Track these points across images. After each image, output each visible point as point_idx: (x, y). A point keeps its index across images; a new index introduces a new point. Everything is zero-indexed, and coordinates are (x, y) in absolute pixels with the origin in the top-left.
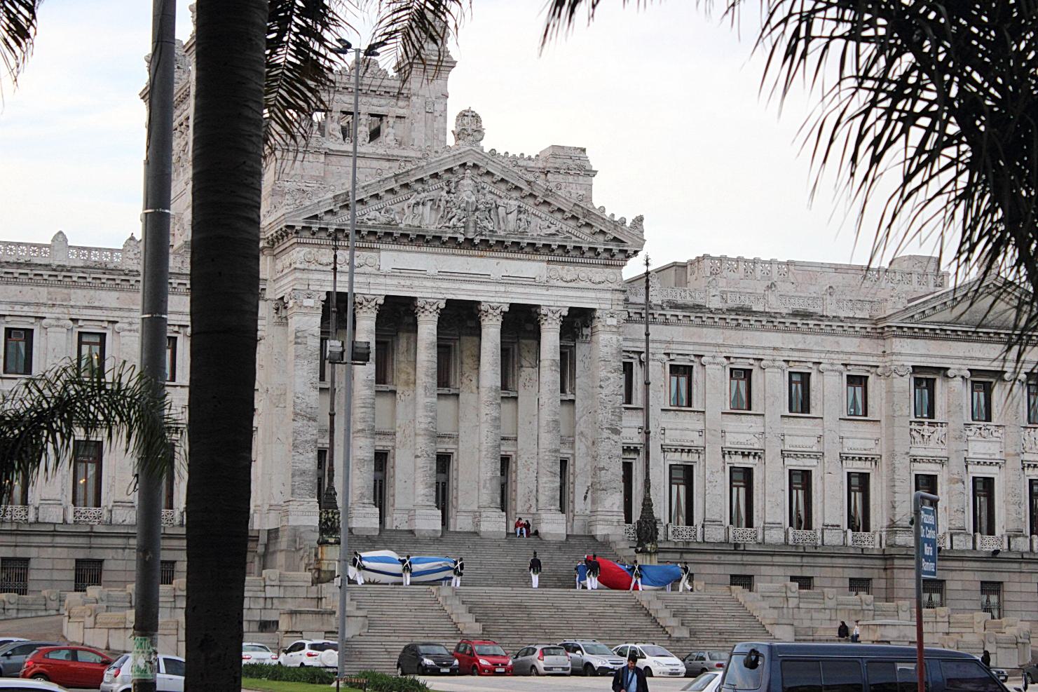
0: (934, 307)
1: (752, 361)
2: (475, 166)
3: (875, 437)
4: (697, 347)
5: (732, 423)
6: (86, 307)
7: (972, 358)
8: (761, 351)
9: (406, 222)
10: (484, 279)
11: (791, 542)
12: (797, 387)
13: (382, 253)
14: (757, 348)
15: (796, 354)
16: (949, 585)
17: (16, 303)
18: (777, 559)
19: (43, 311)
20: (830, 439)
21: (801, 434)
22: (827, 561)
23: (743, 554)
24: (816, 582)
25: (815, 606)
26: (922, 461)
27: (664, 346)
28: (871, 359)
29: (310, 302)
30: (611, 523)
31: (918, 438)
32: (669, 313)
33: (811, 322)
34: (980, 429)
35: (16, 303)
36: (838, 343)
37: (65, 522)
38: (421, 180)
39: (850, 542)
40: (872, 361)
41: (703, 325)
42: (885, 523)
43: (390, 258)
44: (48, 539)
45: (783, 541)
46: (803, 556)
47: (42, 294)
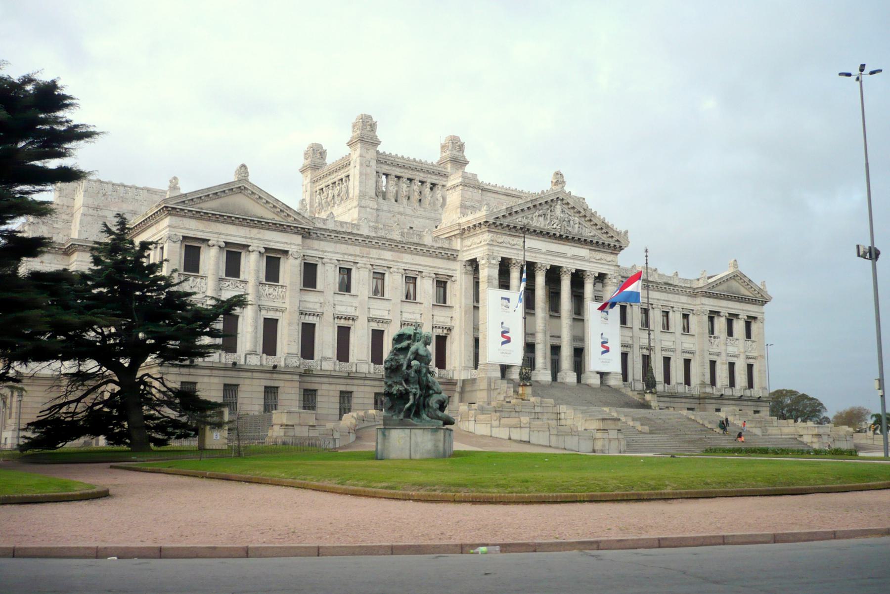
2: (563, 199)
10: (563, 255)
17: (345, 254)
19: (358, 260)
29: (494, 262)
35: (345, 254)
37: (369, 373)
38: (540, 204)
40: (691, 307)
42: (698, 382)
44: (361, 382)
47: (357, 250)
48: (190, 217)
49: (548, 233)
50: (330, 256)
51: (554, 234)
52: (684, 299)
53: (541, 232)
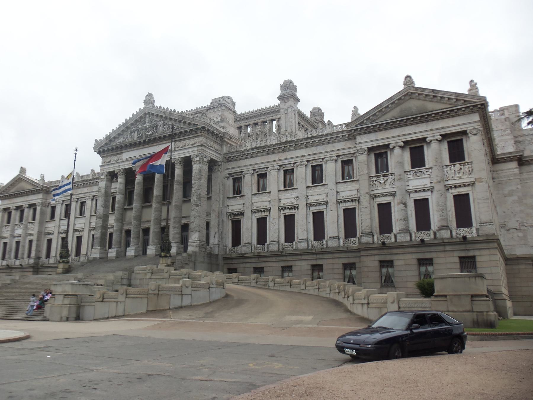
0: (375, 114)
1: (292, 165)
2: (149, 113)
3: (357, 188)
4: (266, 164)
5: (283, 195)
6: (80, 194)
7: (403, 135)
8: (295, 159)
9: (129, 140)
11: (310, 248)
12: (318, 173)
13: (124, 154)
14: (293, 158)
15: (312, 156)
16: (396, 263)
18: (304, 257)
20: (333, 193)
21: (317, 194)
22: (329, 256)
23: (286, 256)
24: (325, 267)
25: (159, 277)
26: (379, 196)
27: (252, 167)
28: (352, 150)
30: (193, 246)
31: (379, 185)
32: (251, 152)
33: (316, 140)
34: (416, 172)
36: (333, 146)
38: (132, 124)
39: (342, 244)
40: (352, 151)
41: (268, 154)
43: (126, 155)
45: (307, 247)
46: (316, 254)
48: (6, 199)
49: (135, 143)
50: (57, 201)
51: (140, 142)
52: (339, 146)
53: (131, 144)
